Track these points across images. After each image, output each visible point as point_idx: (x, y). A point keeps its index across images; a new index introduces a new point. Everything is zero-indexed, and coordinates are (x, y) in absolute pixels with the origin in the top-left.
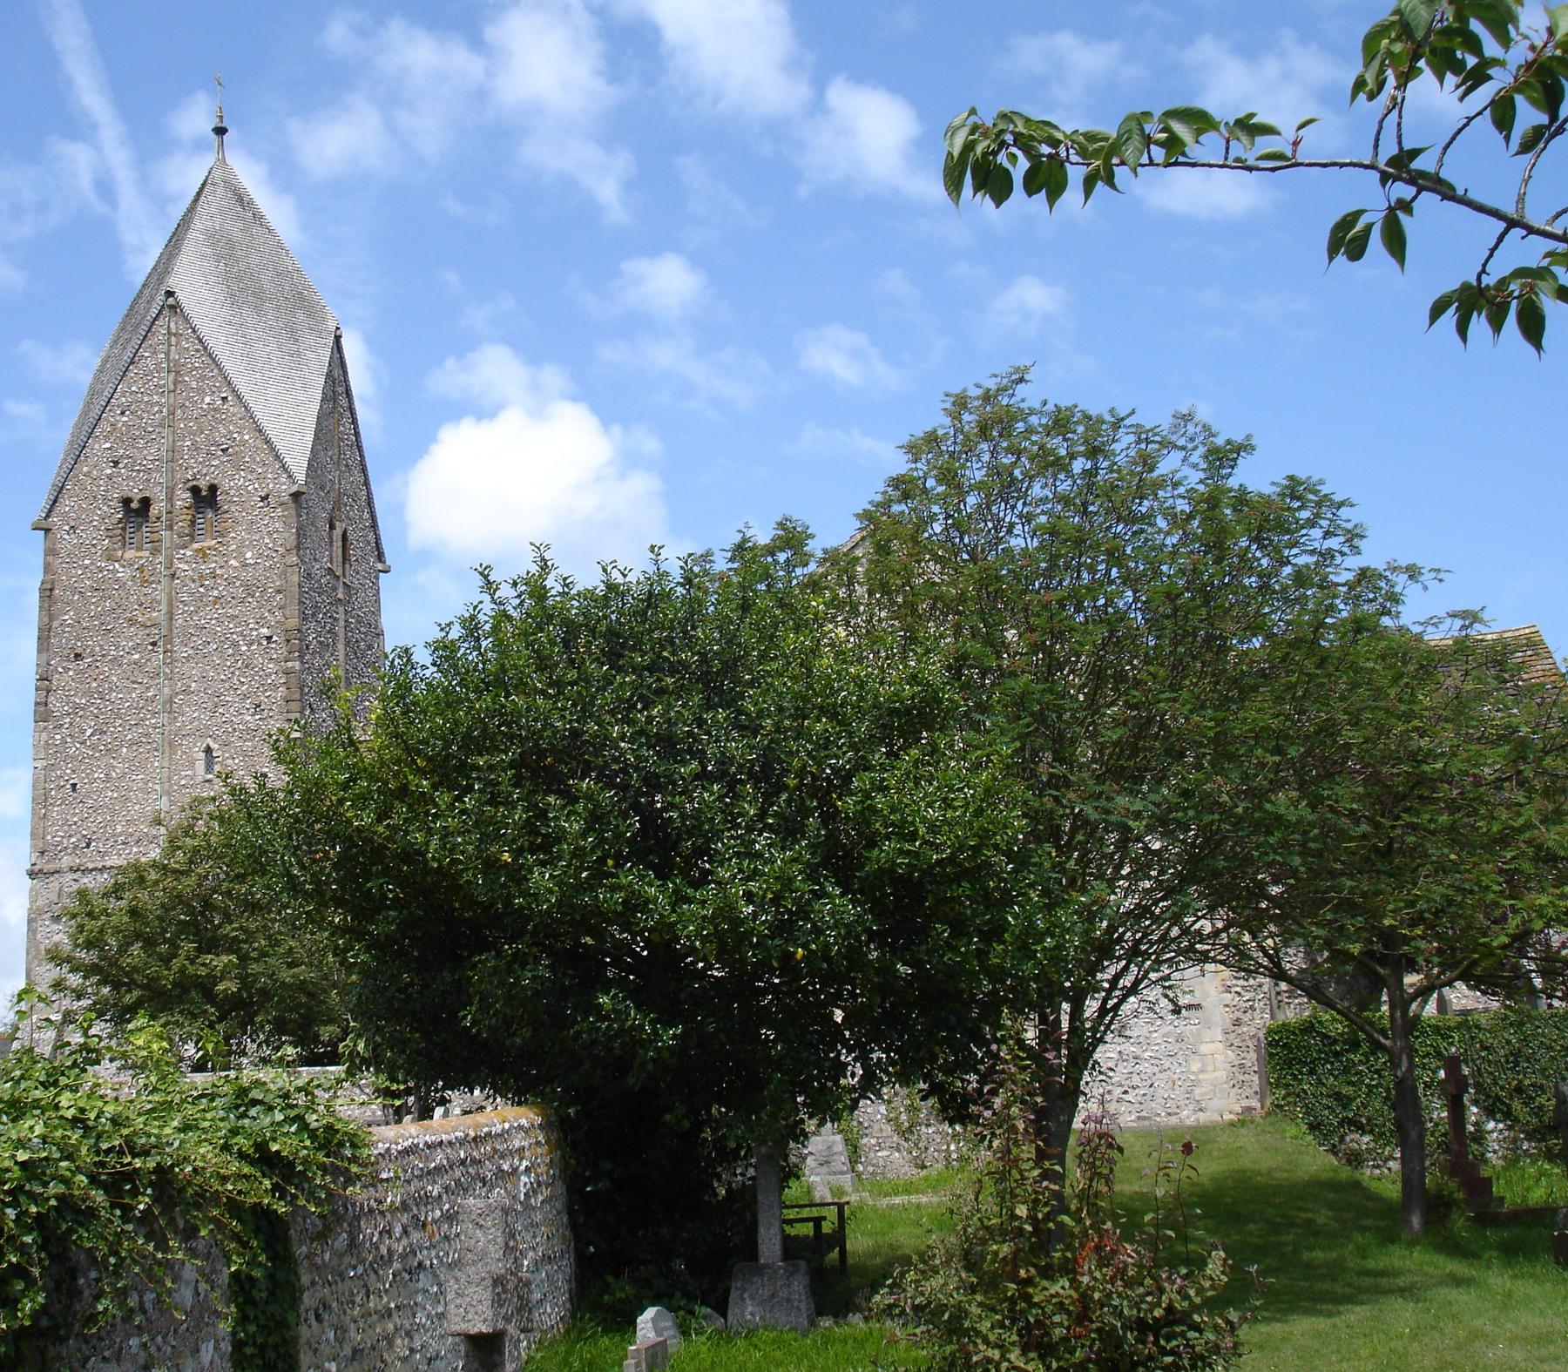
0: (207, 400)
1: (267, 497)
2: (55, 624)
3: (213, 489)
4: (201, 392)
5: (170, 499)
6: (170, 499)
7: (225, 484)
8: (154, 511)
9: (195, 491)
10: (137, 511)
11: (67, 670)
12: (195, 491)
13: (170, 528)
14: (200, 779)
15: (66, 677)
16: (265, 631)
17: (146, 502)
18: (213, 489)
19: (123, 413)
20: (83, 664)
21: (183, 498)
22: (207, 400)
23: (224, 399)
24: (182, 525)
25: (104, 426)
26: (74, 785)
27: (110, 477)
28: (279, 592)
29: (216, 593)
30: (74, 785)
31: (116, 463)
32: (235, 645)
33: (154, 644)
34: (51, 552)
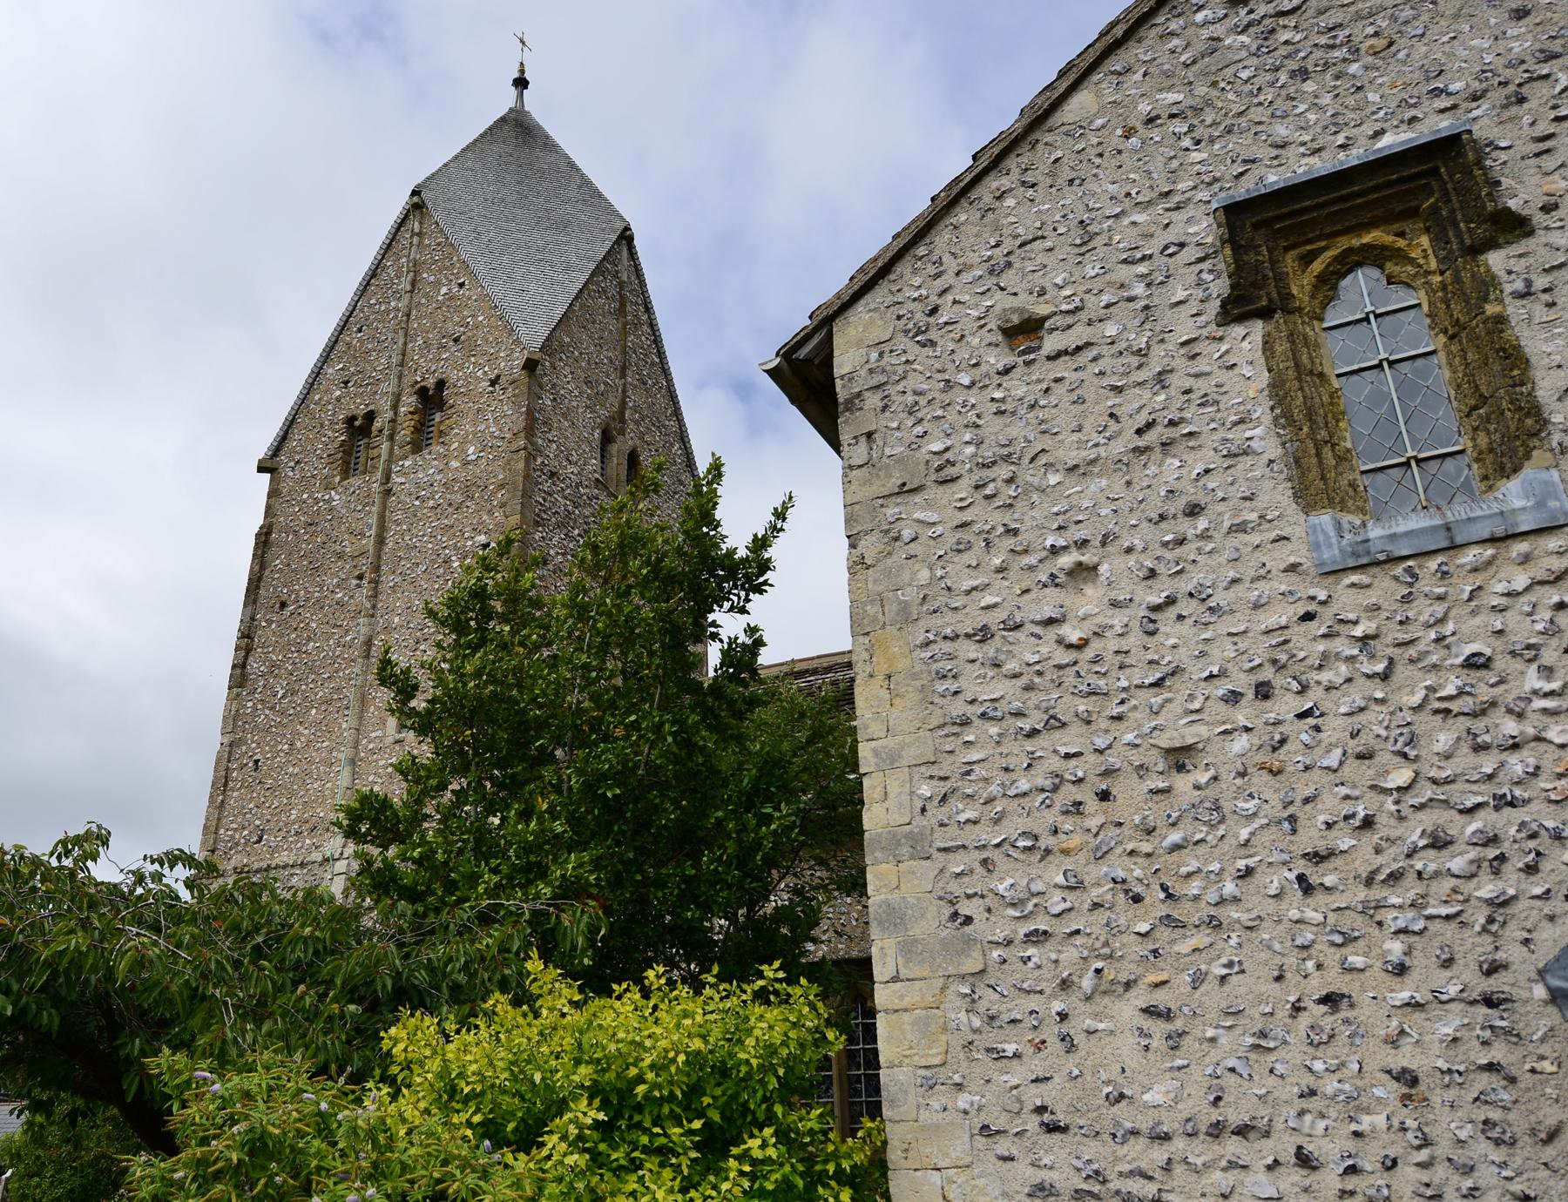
0: (444, 290)
1: (498, 377)
2: (267, 572)
3: (441, 384)
4: (438, 284)
5: (395, 407)
6: (395, 407)
7: (453, 376)
8: (377, 424)
9: (422, 393)
10: (360, 428)
11: (270, 622)
12: (422, 393)
13: (391, 438)
14: (390, 740)
15: (266, 634)
16: (482, 539)
17: (370, 416)
18: (441, 384)
19: (360, 330)
20: (287, 612)
21: (409, 402)
22: (444, 290)
23: (461, 285)
24: (404, 434)
25: (340, 347)
26: (257, 762)
27: (338, 399)
28: (502, 486)
29: (431, 503)
30: (257, 762)
31: (346, 383)
32: (447, 561)
33: (360, 577)
34: (273, 493)
